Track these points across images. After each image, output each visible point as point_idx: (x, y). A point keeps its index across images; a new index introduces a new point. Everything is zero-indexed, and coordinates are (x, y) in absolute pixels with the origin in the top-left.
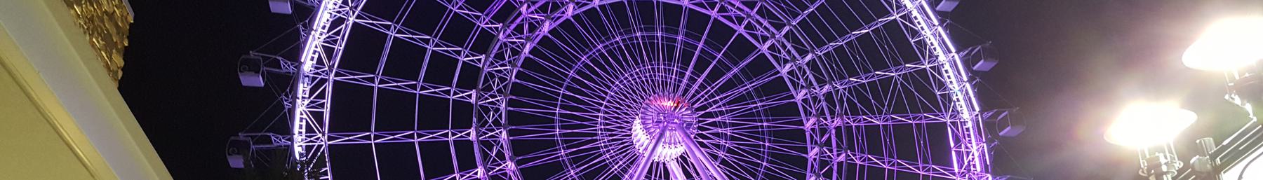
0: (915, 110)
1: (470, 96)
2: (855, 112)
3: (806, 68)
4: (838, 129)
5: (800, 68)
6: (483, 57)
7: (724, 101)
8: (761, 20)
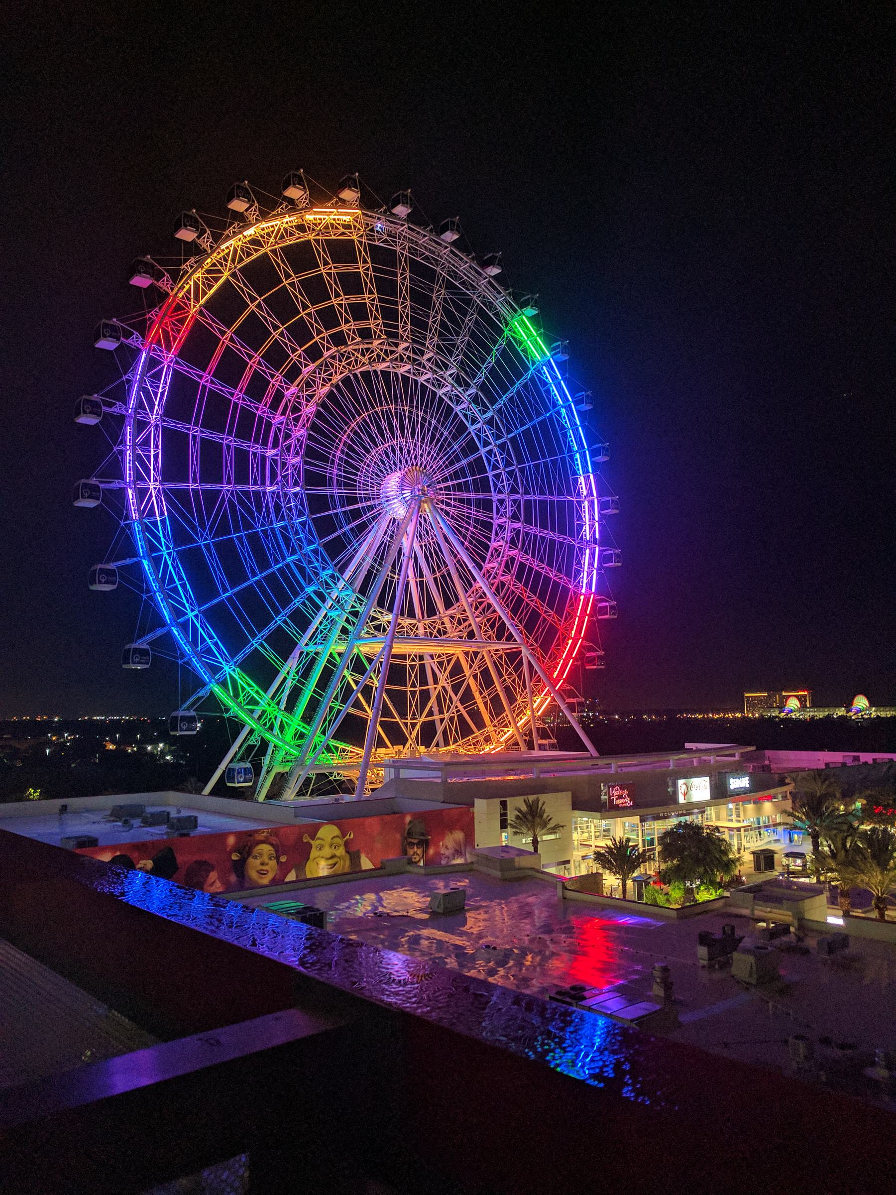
1: (328, 349)
6: (358, 339)
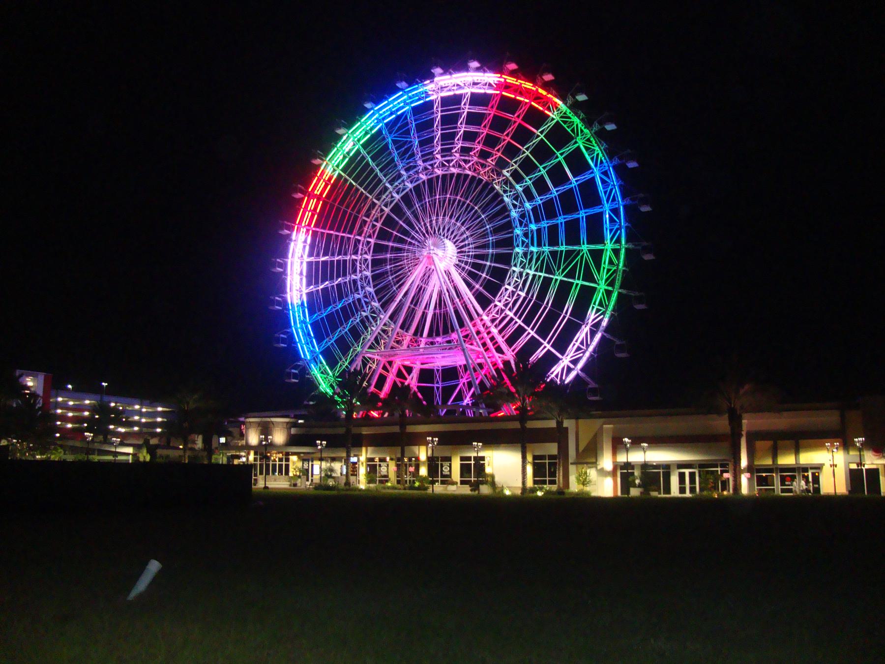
0: (407, 124)
2: (413, 155)
3: (394, 185)
4: (424, 161)
5: (394, 189)
7: (419, 225)
8: (372, 215)
